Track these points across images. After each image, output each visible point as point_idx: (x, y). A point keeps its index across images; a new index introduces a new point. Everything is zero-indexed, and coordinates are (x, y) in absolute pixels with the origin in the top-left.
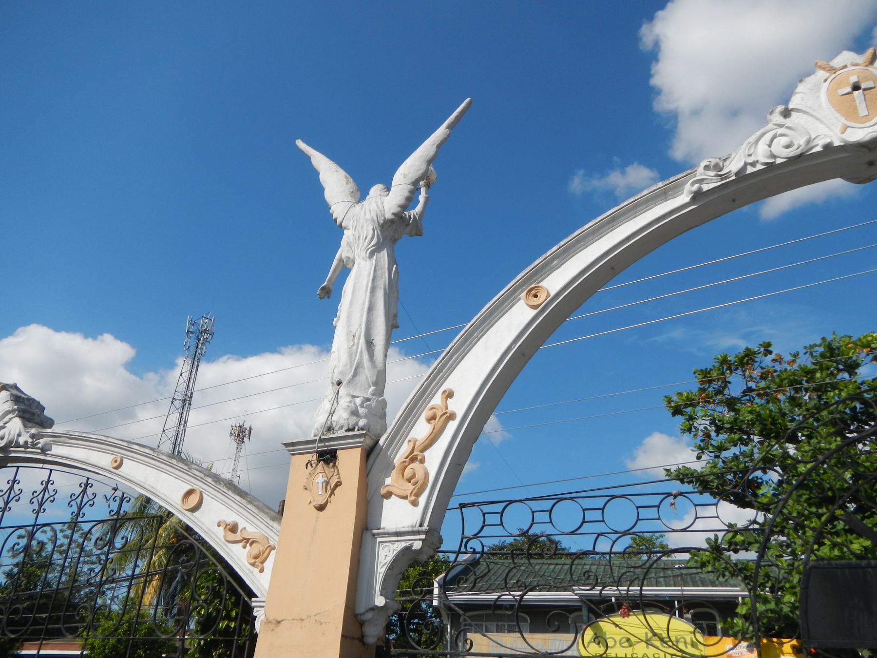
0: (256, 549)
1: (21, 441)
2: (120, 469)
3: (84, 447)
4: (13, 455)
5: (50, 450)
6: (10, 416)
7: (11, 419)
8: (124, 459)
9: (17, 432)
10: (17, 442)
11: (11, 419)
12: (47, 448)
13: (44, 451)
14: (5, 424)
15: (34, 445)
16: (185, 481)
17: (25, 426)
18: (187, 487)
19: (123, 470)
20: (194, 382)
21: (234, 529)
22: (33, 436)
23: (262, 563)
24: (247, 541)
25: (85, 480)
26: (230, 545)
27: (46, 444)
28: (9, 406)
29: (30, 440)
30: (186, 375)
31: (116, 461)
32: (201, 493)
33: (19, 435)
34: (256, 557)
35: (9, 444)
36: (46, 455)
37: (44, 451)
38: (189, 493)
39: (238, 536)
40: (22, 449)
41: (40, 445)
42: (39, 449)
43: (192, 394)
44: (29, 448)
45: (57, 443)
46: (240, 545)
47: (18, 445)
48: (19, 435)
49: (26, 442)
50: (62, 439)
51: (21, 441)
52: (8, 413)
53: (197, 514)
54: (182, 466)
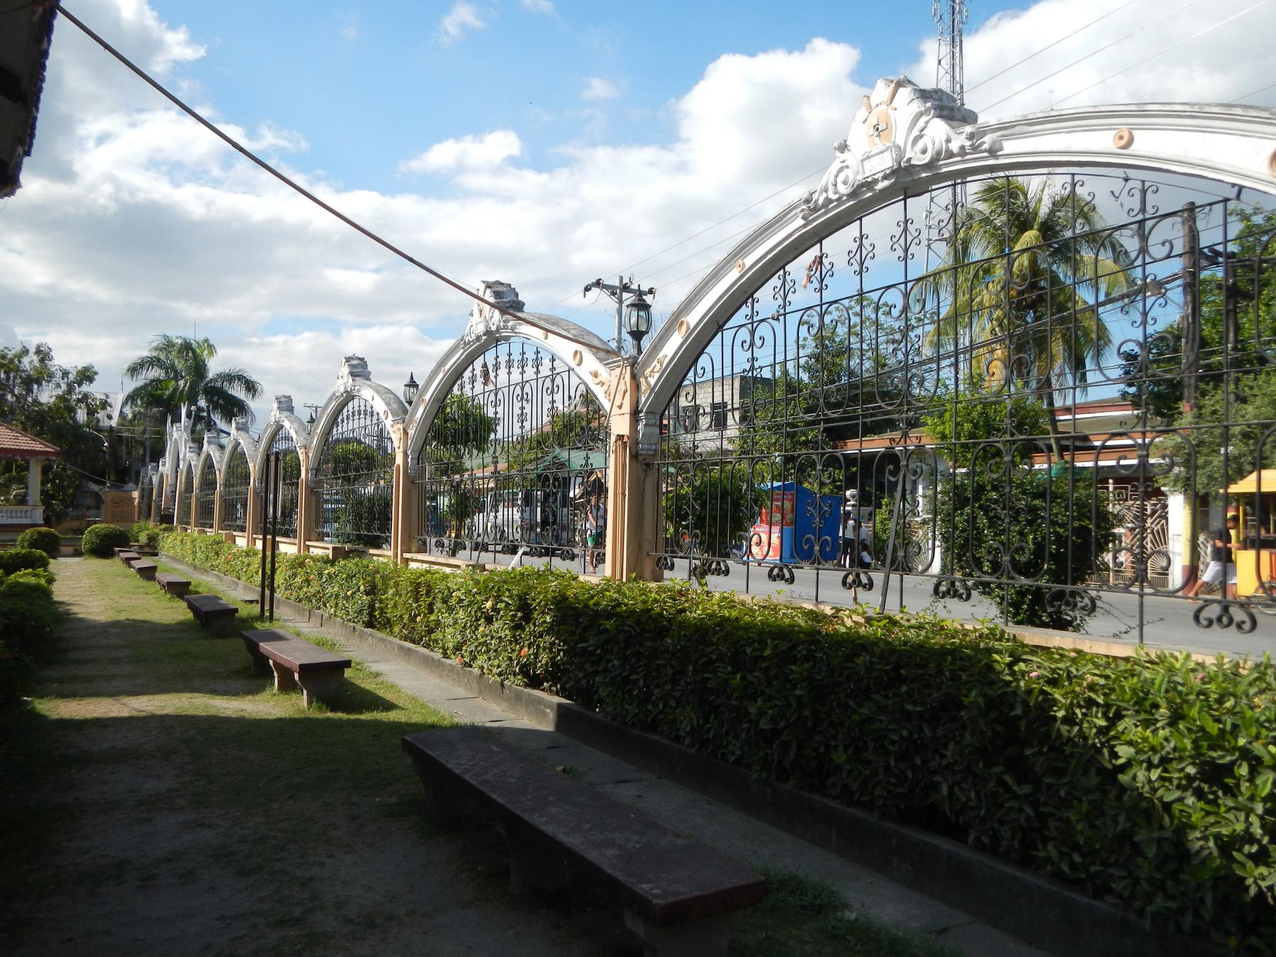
1: (954, 147)
2: (1133, 147)
3: (1057, 131)
4: (944, 170)
5: (1002, 149)
6: (924, 119)
7: (927, 122)
8: (1135, 133)
9: (944, 138)
10: (948, 150)
11: (927, 122)
12: (997, 147)
13: (993, 152)
14: (922, 131)
15: (975, 149)
19: (1136, 148)
20: (961, 68)
22: (971, 137)
25: (1068, 179)
27: (994, 143)
28: (917, 106)
29: (968, 143)
30: (946, 63)
31: (1121, 138)
33: (948, 141)
35: (937, 157)
36: (997, 157)
37: (993, 152)
40: (959, 159)
41: (986, 146)
42: (985, 151)
43: (962, 87)
44: (967, 154)
45: (1008, 137)
47: (951, 155)
48: (948, 141)
49: (963, 148)
50: (1017, 129)
51: (954, 147)
52: (920, 114)
54: (1255, 114)
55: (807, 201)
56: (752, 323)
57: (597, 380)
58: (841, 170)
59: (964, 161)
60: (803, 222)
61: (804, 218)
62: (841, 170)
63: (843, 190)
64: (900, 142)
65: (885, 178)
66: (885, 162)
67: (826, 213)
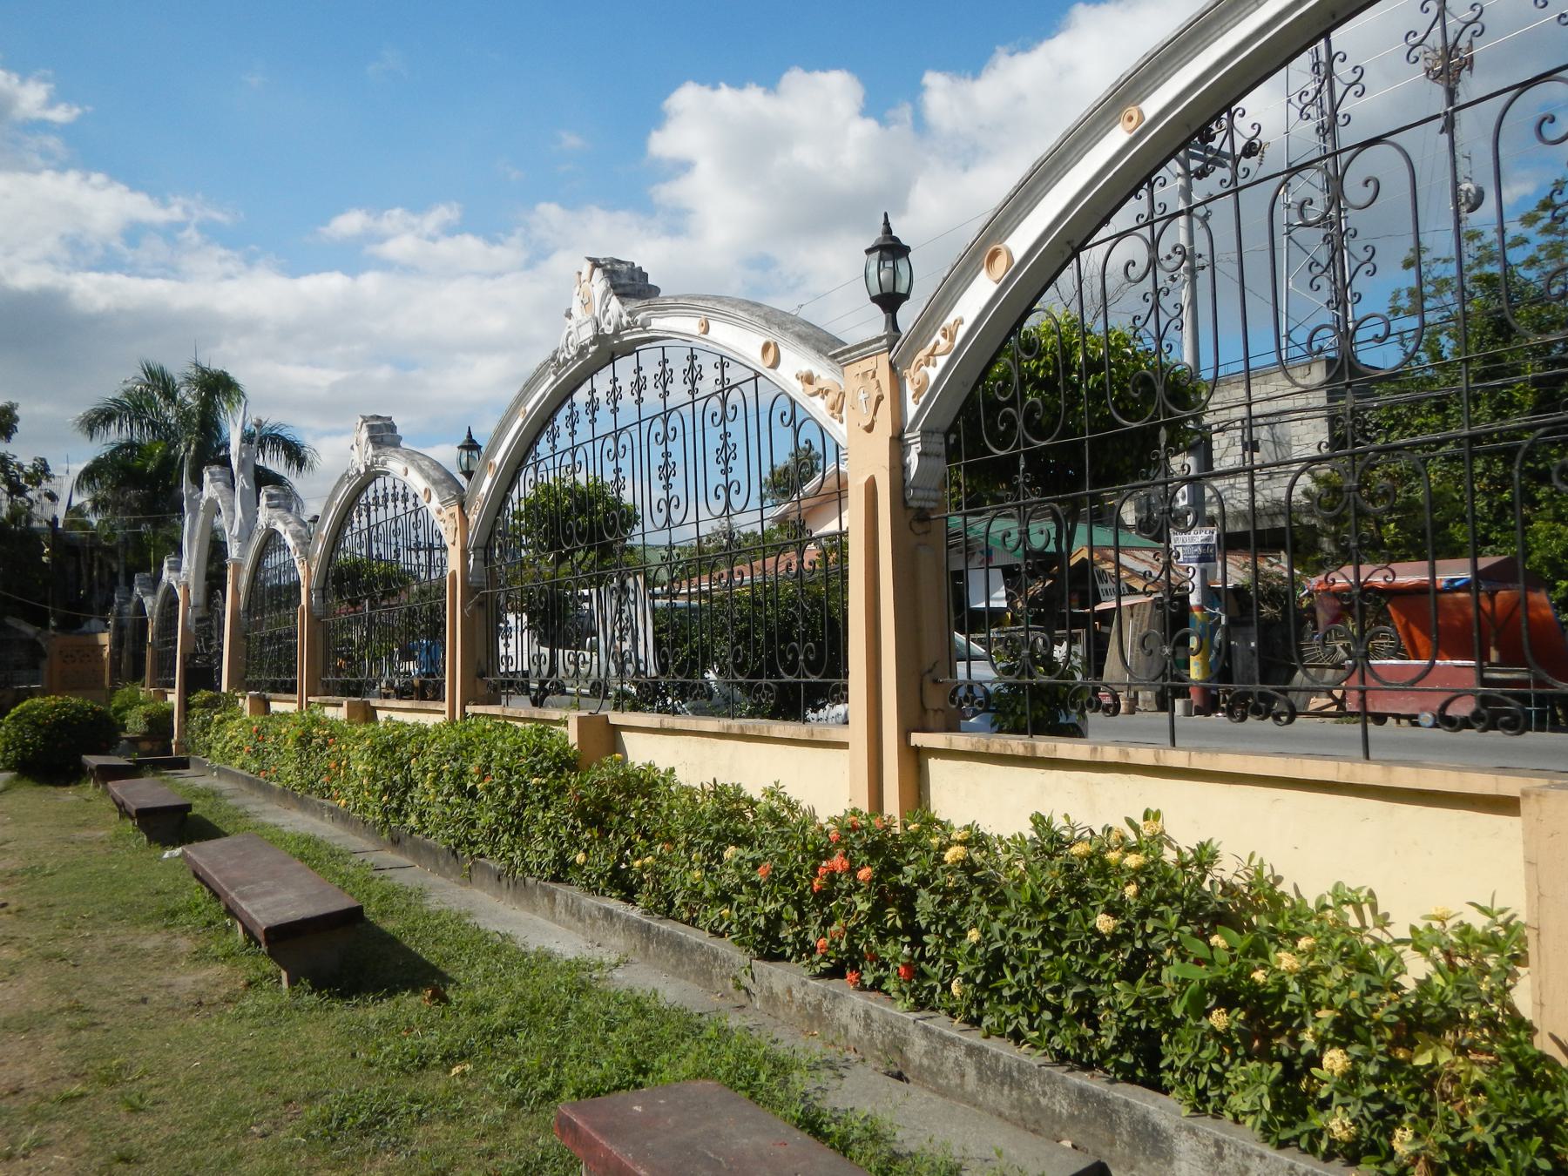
0: (831, 398)
13: (643, 326)
16: (761, 334)
17: (623, 304)
18: (762, 341)
19: (712, 335)
21: (809, 379)
23: (840, 411)
24: (824, 392)
26: (814, 399)
27: (643, 320)
32: (776, 344)
33: (621, 316)
34: (833, 408)
36: (648, 332)
37: (643, 326)
38: (766, 348)
39: (813, 389)
46: (818, 397)
53: (779, 370)
55: (553, 359)
56: (723, 391)
57: (440, 517)
58: (570, 333)
59: (633, 333)
60: (553, 378)
61: (555, 373)
62: (570, 333)
63: (573, 352)
64: (597, 314)
65: (592, 343)
66: (587, 333)
67: (567, 370)
